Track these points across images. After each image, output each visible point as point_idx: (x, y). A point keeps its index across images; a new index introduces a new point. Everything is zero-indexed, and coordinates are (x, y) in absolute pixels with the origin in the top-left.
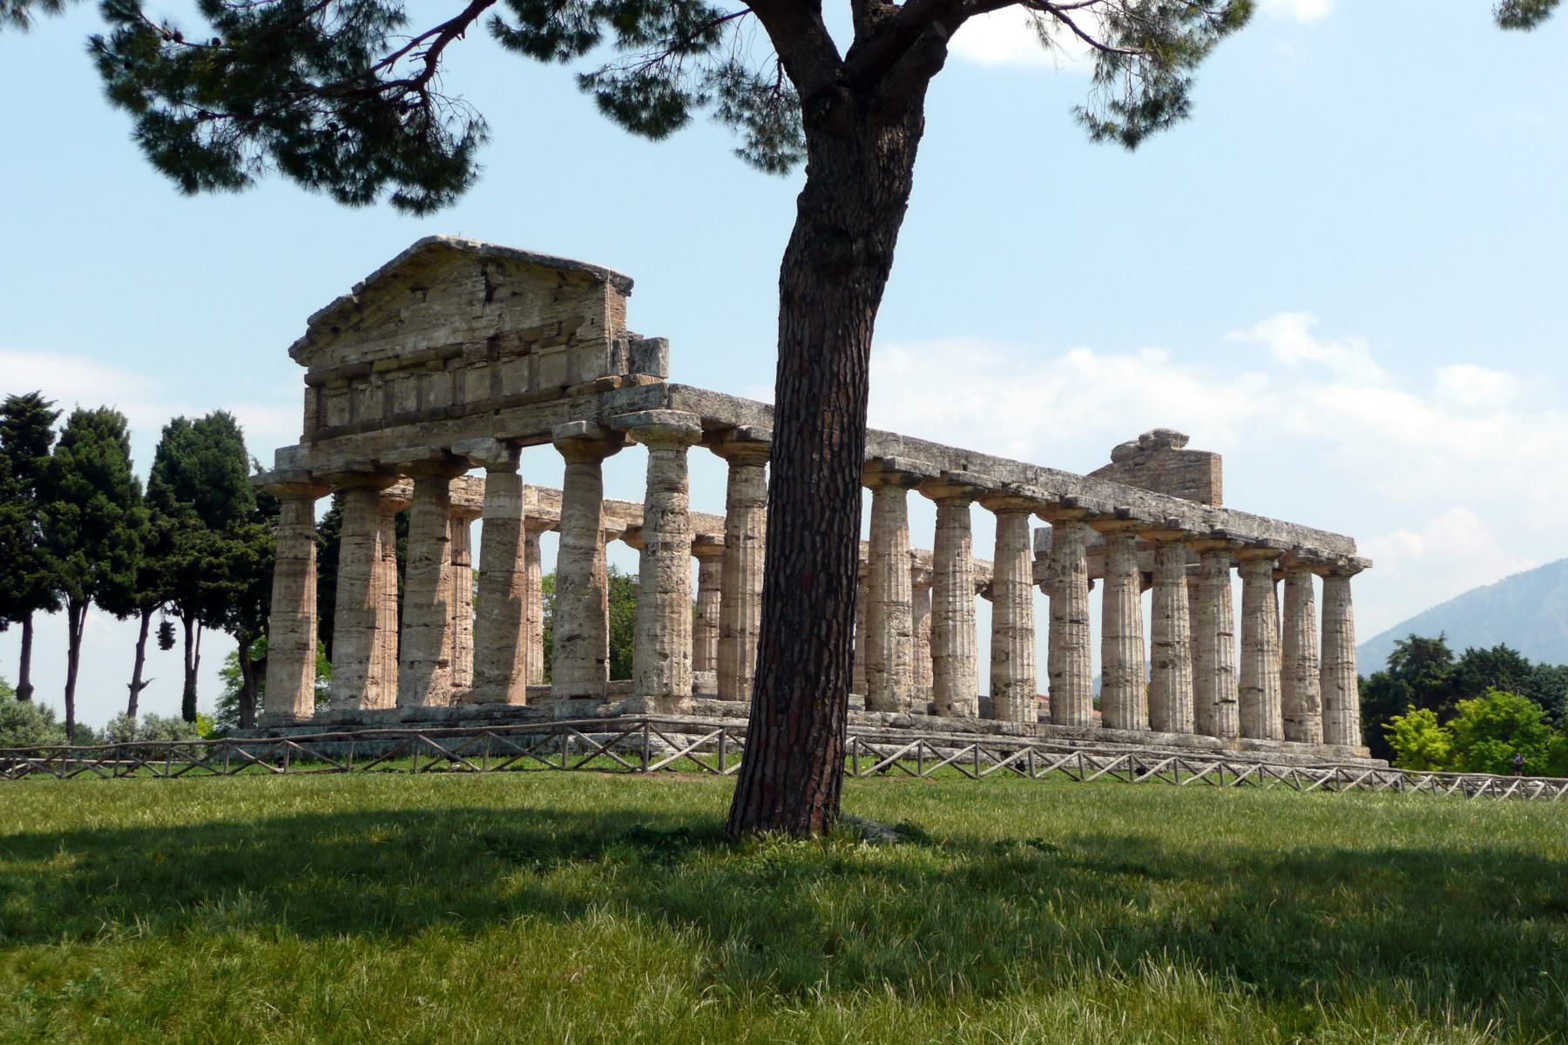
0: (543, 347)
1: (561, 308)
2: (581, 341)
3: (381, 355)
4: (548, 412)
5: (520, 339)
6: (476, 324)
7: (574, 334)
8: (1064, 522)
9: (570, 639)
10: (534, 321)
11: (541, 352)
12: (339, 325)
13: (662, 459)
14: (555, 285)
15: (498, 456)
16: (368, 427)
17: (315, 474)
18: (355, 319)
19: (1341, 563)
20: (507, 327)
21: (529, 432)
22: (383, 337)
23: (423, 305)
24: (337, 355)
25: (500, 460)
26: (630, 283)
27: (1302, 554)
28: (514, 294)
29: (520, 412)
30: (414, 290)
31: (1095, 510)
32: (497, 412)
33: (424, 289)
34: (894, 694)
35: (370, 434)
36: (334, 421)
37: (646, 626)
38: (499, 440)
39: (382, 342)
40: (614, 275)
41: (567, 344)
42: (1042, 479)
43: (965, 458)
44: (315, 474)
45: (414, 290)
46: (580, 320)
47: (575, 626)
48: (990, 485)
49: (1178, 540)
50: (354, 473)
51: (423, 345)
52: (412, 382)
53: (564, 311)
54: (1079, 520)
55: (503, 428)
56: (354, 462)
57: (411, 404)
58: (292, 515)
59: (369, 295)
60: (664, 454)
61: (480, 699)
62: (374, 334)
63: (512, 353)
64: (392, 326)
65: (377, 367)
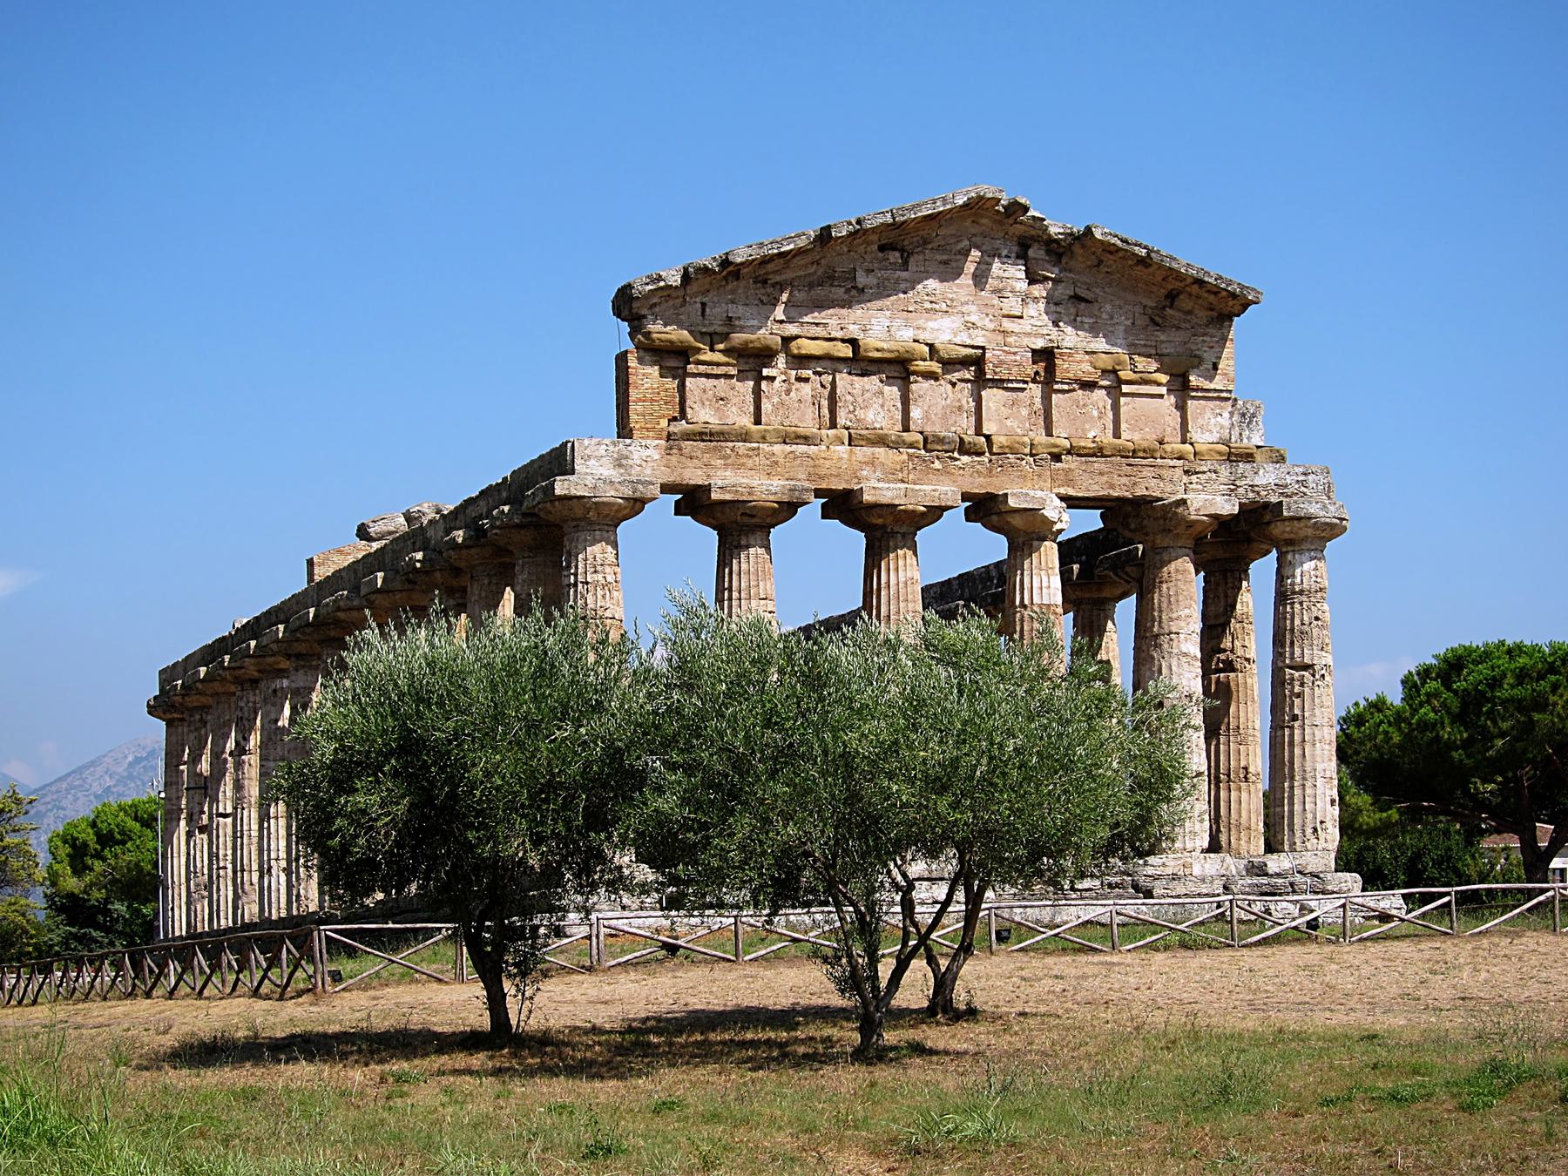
1: (1163, 338)
4: (1147, 472)
6: (1008, 325)
11: (1125, 389)
14: (1151, 304)
23: (904, 274)
28: (1077, 298)
29: (1099, 464)
30: (882, 248)
32: (1056, 458)
35: (802, 448)
36: (702, 414)
45: (882, 248)
51: (908, 334)
52: (873, 382)
55: (1069, 482)
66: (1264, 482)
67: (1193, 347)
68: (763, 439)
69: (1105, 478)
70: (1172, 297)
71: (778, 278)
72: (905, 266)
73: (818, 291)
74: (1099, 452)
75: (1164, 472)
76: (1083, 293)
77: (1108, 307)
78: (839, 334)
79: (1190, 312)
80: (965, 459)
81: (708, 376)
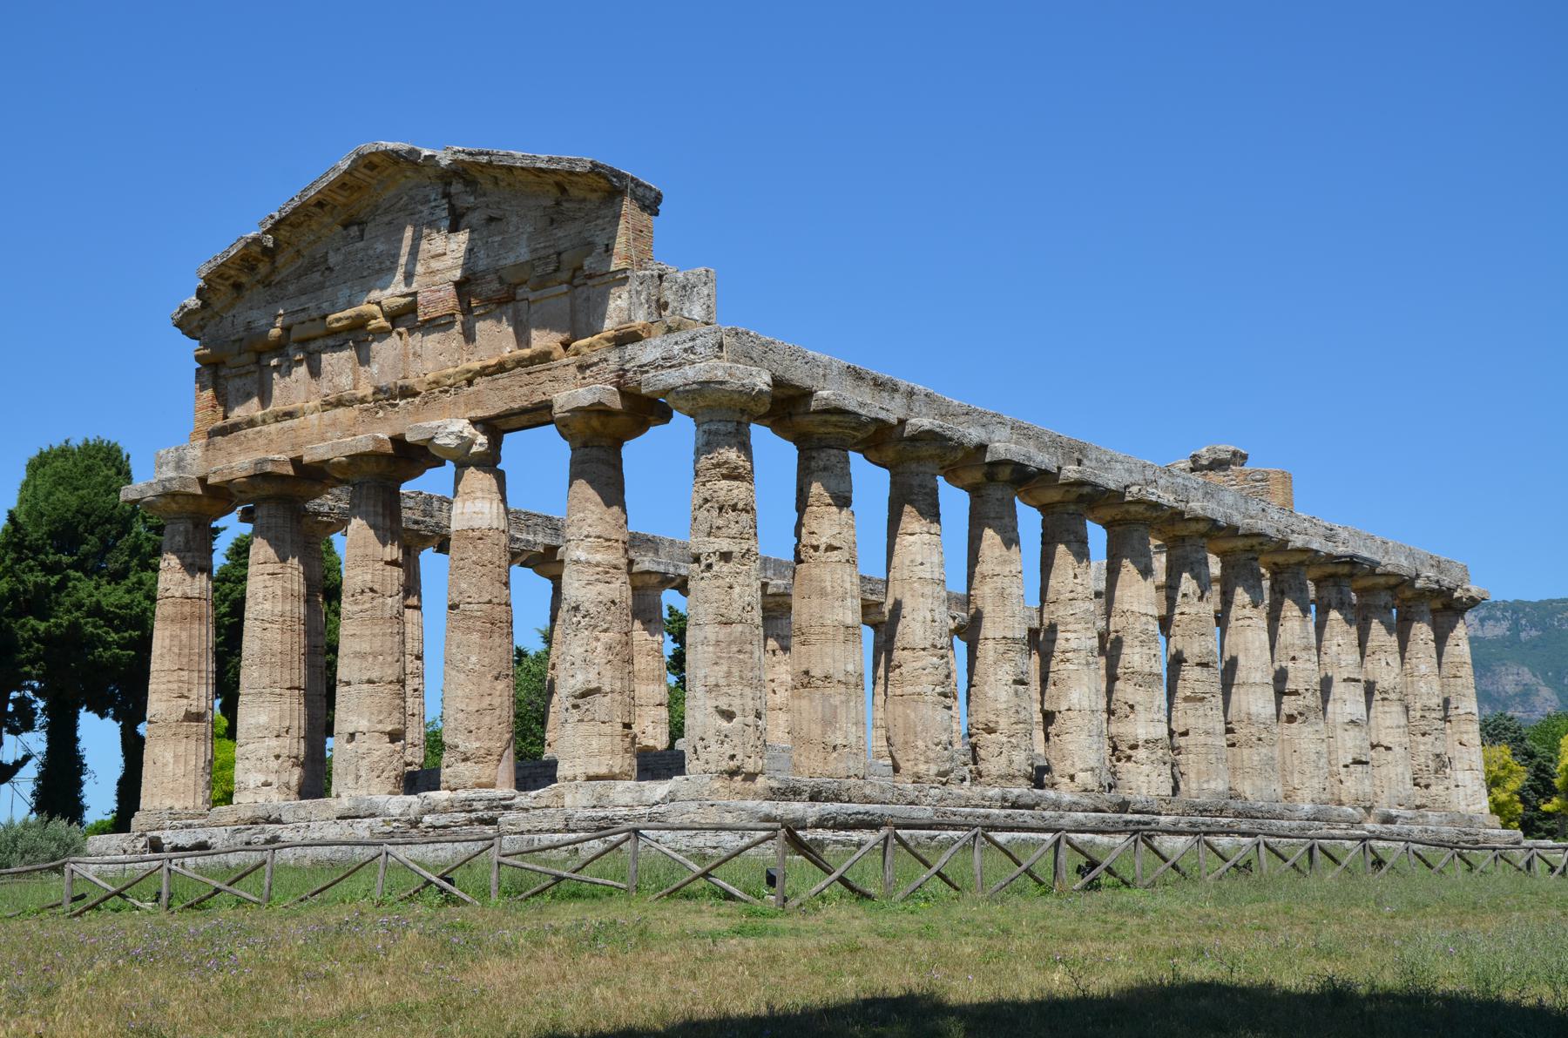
0: (534, 290)
2: (590, 277)
3: (302, 316)
4: (544, 376)
5: (501, 280)
6: (435, 265)
7: (581, 268)
8: (1183, 538)
9: (585, 694)
10: (523, 253)
12: (244, 279)
13: (716, 433)
15: (472, 442)
16: (290, 415)
17: (210, 481)
18: (263, 268)
19: (1456, 595)
20: (482, 263)
21: (516, 406)
22: (303, 292)
23: (360, 245)
24: (240, 320)
25: (475, 449)
26: (658, 198)
27: (1419, 584)
28: (491, 219)
29: (503, 379)
30: (346, 226)
31: (1222, 523)
32: (470, 383)
33: (361, 224)
34: (1011, 762)
35: (289, 423)
37: (701, 674)
38: (474, 422)
39: (304, 298)
40: (638, 184)
41: (570, 283)
42: (1162, 482)
43: (1078, 453)
44: (210, 481)
45: (346, 226)
46: (589, 246)
47: (592, 676)
48: (1112, 486)
49: (1301, 563)
50: (267, 476)
53: (565, 235)
54: (1203, 535)
55: (479, 404)
56: (266, 461)
57: (345, 381)
58: (179, 539)
59: (284, 233)
60: (722, 427)
61: (452, 783)
62: (292, 288)
63: (489, 300)
64: (316, 277)
65: (296, 334)
66: (650, 358)
67: (586, 234)
68: (264, 422)
69: (507, 393)
70: (563, 190)
71: (278, 278)
72: (362, 237)
73: (304, 280)
74: (501, 368)
75: (556, 373)
76: (495, 213)
77: (514, 219)
78: (315, 315)
79: (584, 200)
80: (402, 403)
81: (240, 376)
